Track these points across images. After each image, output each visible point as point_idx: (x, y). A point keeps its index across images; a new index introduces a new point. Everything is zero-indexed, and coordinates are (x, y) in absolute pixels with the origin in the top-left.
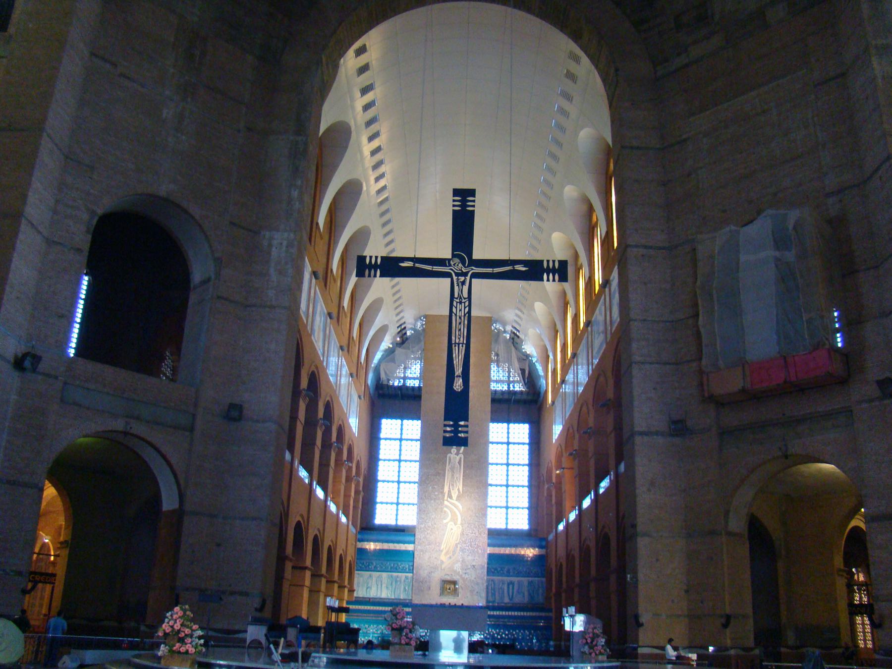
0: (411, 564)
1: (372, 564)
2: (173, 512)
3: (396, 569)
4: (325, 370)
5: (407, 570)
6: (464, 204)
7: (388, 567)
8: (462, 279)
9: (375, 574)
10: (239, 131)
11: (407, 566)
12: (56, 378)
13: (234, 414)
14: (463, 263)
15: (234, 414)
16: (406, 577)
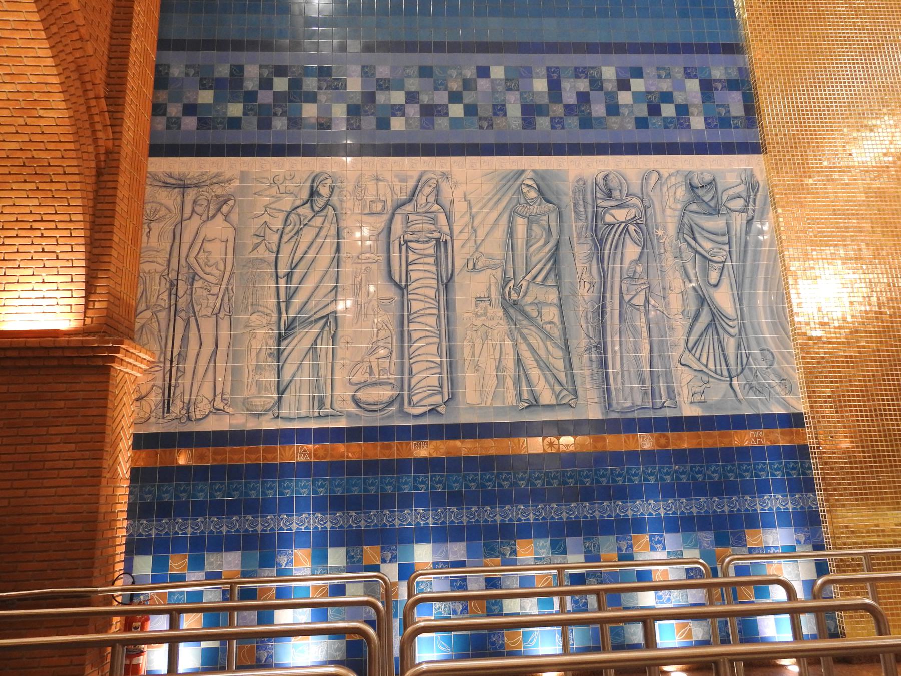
3: (586, 122)
5: (697, 122)
7: (500, 109)
11: (693, 85)
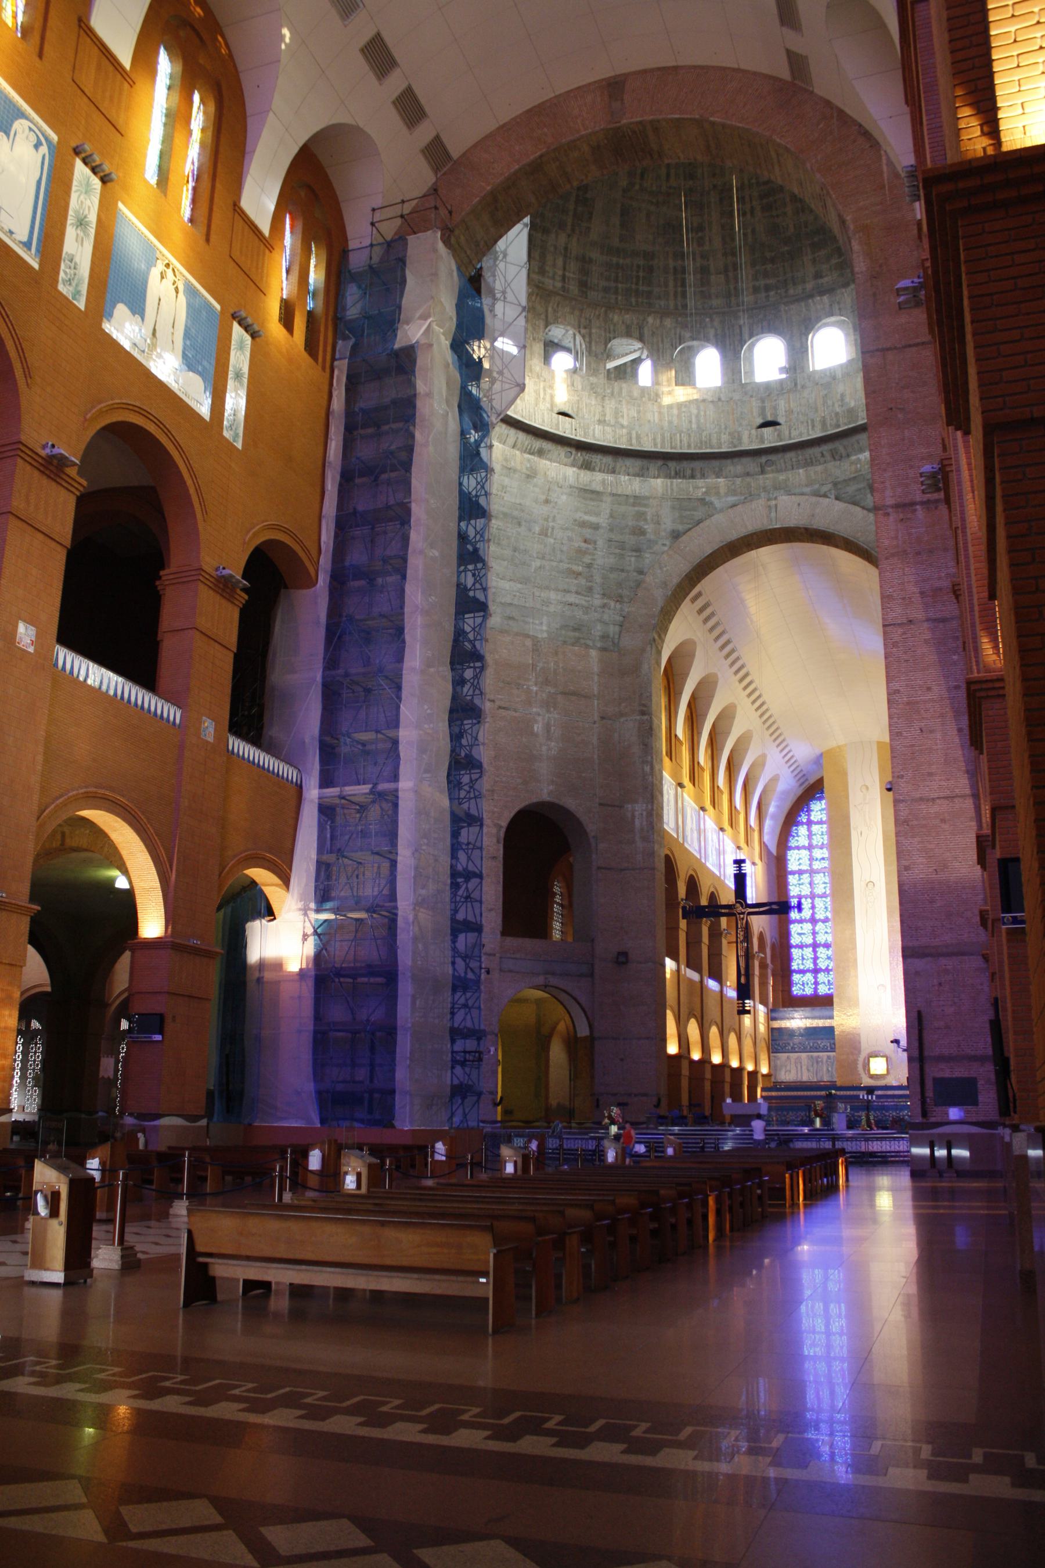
0: (832, 1042)
1: (789, 1044)
2: (586, 1037)
4: (704, 866)
6: (740, 868)
8: (742, 916)
9: (794, 1056)
10: (595, 723)
12: (494, 955)
13: (622, 959)
14: (742, 906)
15: (622, 959)
16: (829, 1057)
